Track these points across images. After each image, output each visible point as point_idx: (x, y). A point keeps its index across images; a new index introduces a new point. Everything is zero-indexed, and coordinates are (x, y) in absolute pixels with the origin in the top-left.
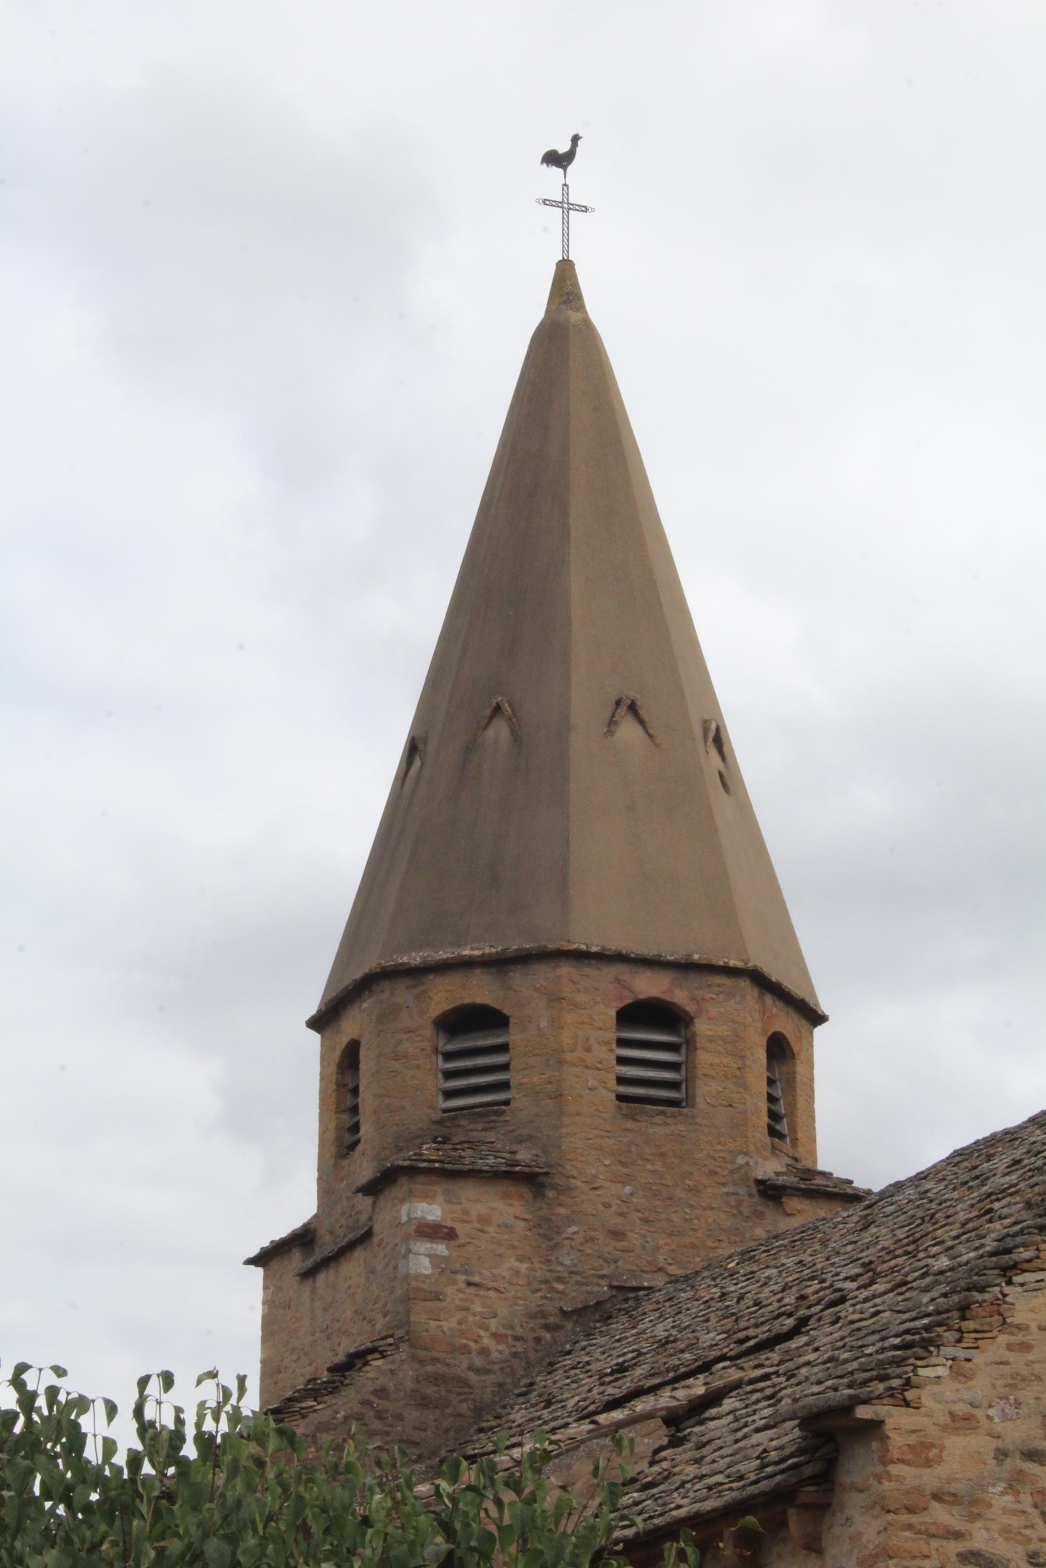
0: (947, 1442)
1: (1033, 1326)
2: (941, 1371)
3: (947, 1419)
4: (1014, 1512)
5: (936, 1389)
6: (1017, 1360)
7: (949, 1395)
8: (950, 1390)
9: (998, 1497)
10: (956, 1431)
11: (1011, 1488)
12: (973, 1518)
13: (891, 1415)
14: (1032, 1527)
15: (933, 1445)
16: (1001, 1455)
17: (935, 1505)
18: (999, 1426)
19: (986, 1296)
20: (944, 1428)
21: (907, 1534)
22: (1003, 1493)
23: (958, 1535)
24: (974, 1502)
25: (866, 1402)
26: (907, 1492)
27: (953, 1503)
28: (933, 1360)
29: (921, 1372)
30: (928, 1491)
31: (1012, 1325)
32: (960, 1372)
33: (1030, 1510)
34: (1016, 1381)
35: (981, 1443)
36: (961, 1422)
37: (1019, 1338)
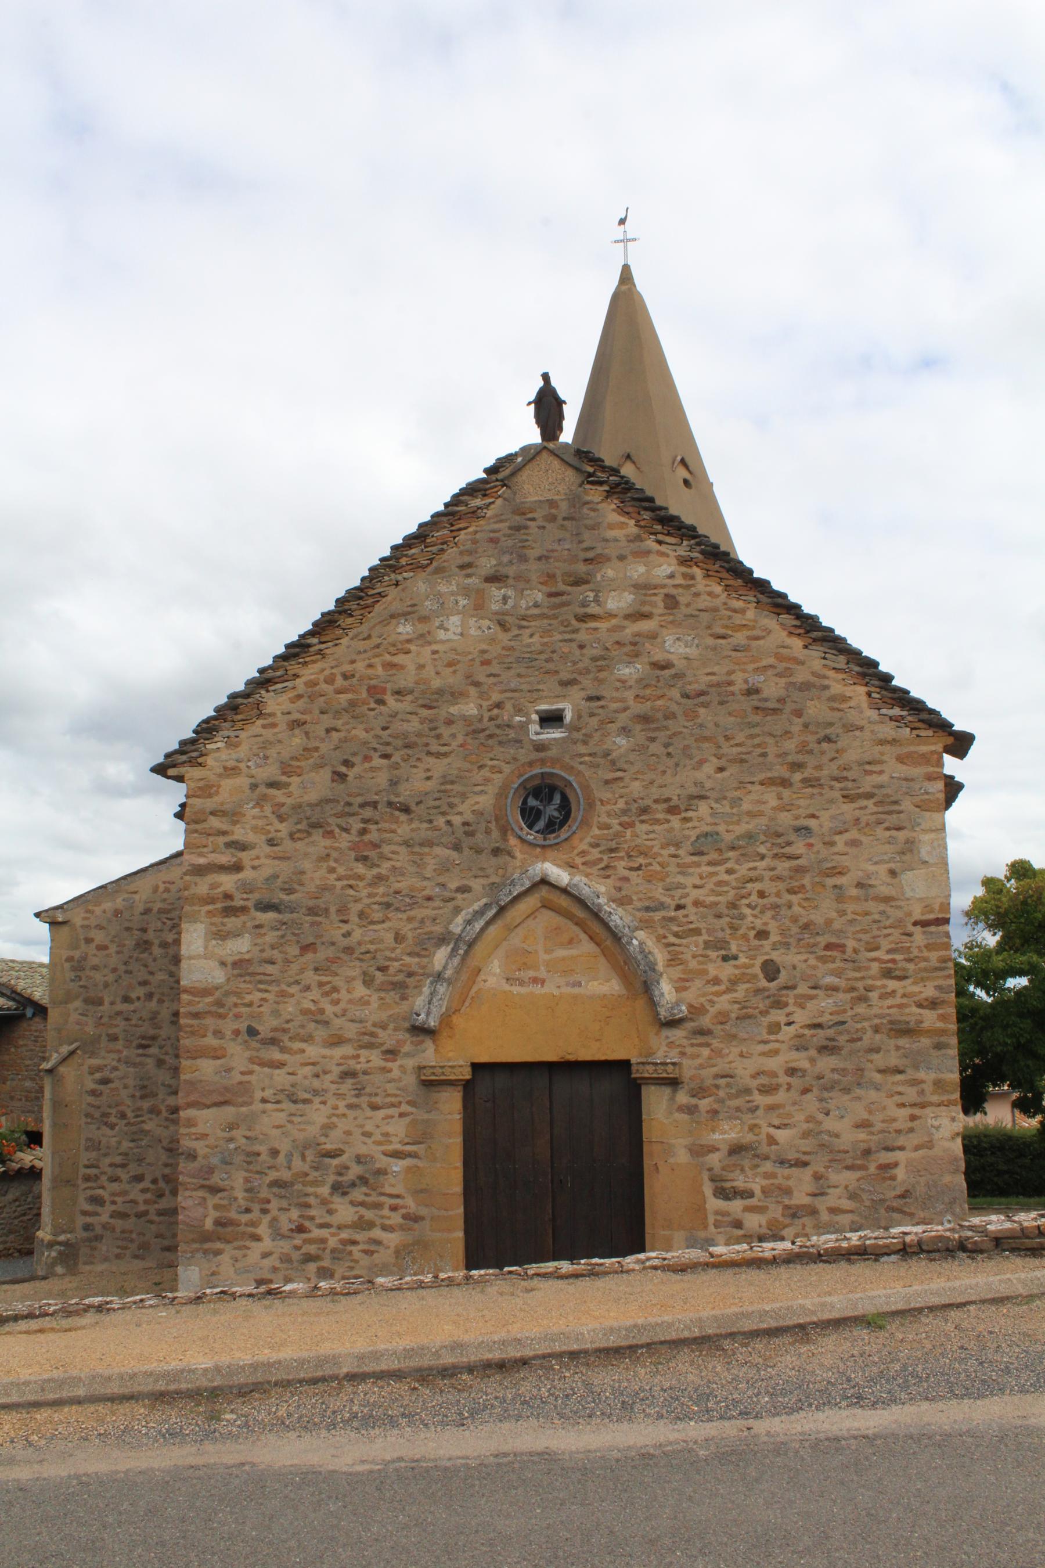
0: (223, 783)
1: (279, 714)
2: (219, 745)
3: (222, 770)
4: (259, 818)
5: (217, 755)
6: (268, 734)
7: (224, 757)
8: (224, 755)
9: (250, 811)
10: (228, 776)
11: (258, 804)
12: (235, 823)
13: (188, 772)
14: (271, 824)
15: (213, 786)
16: (254, 787)
17: (212, 818)
18: (254, 772)
19: (250, 700)
20: (220, 775)
21: (196, 835)
22: (253, 808)
23: (224, 833)
24: (234, 814)
25: (174, 766)
26: (195, 813)
27: (223, 816)
28: (216, 739)
29: (208, 746)
30: (208, 810)
31: (265, 714)
32: (232, 744)
33: (269, 815)
34: (266, 745)
35: (243, 781)
36: (231, 771)
37: (270, 720)
